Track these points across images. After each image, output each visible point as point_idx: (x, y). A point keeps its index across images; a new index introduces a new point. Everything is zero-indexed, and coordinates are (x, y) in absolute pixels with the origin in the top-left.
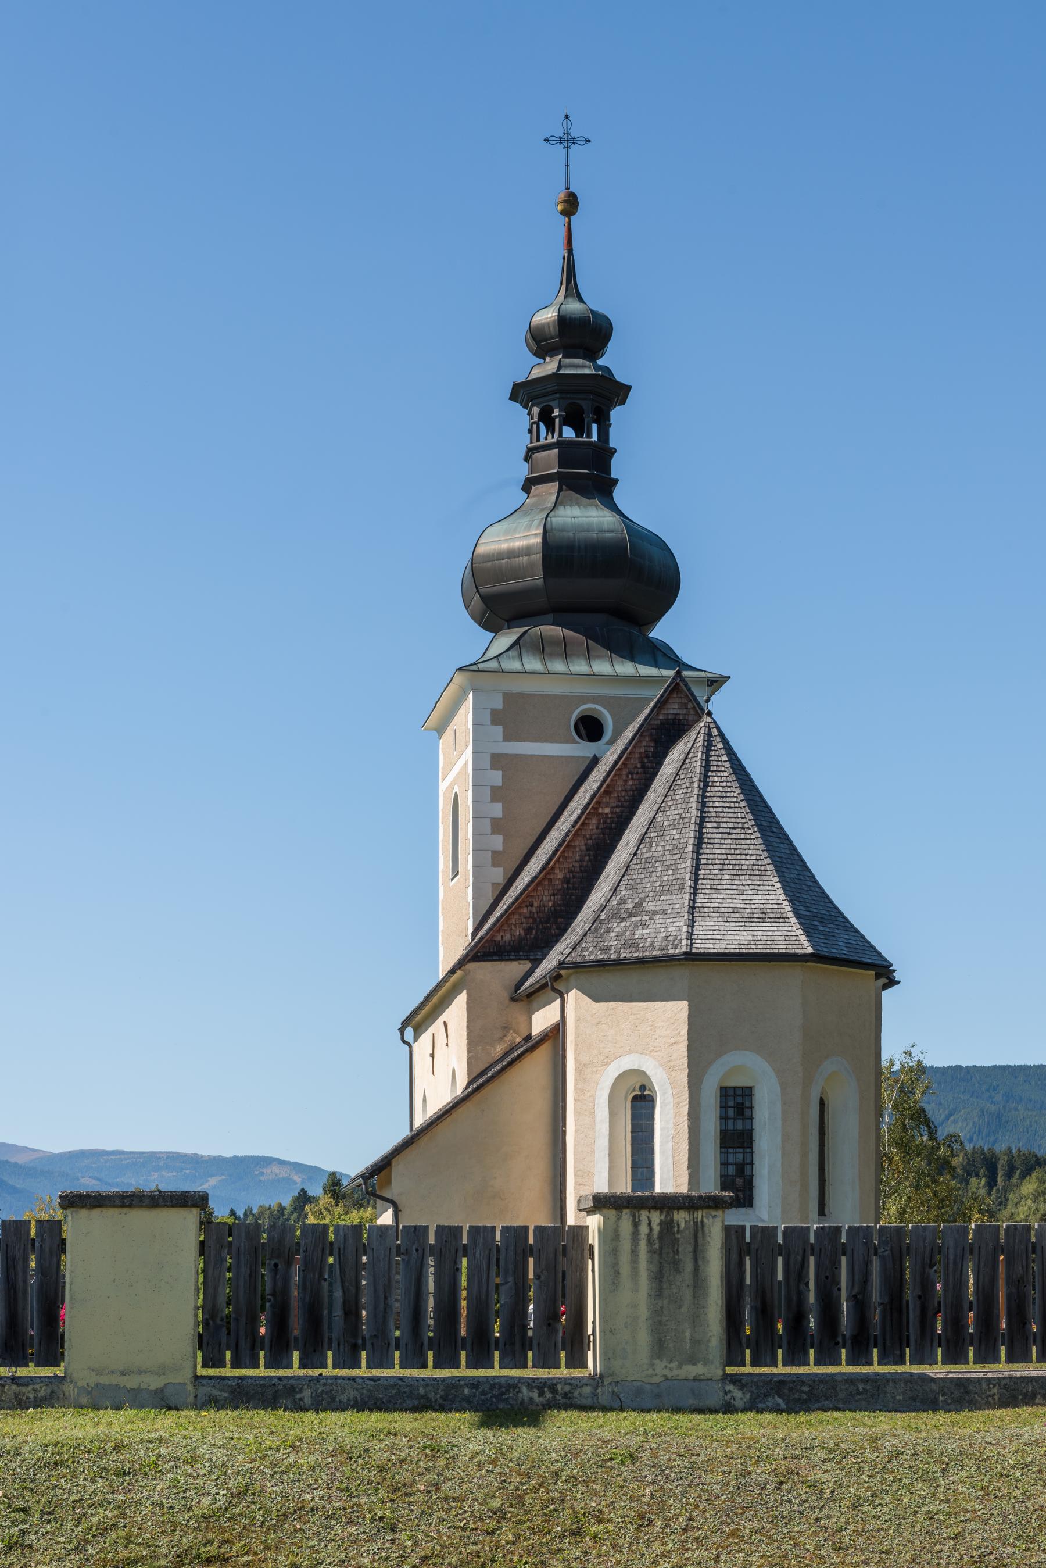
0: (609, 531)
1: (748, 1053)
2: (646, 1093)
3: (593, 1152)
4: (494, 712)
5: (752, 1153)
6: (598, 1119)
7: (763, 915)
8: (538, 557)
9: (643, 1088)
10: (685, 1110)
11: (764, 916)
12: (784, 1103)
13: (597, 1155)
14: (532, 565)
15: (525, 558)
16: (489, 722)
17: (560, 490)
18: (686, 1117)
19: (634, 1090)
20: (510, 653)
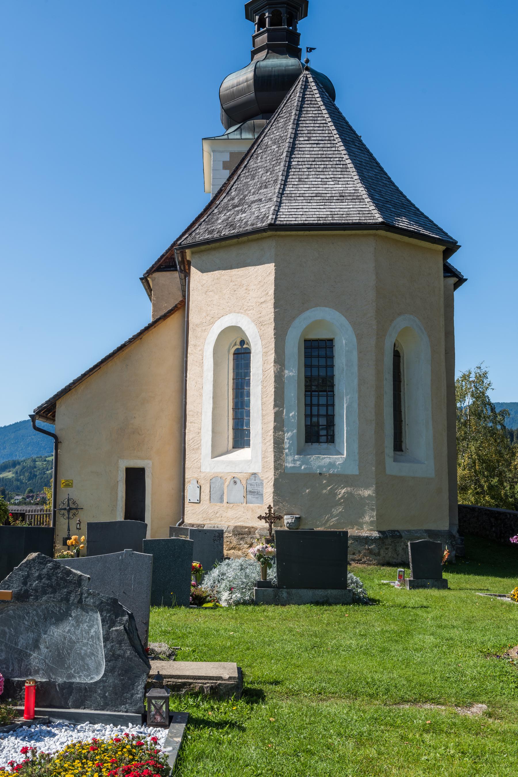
0: (292, 66)
1: (327, 309)
2: (245, 346)
3: (201, 395)
4: (224, 163)
5: (333, 396)
6: (205, 368)
7: (342, 197)
8: (252, 81)
9: (242, 342)
10: (272, 357)
11: (342, 198)
12: (360, 352)
13: (204, 398)
14: (248, 86)
15: (245, 84)
16: (222, 169)
17: (268, 53)
18: (273, 364)
19: (235, 344)
20: (235, 132)
